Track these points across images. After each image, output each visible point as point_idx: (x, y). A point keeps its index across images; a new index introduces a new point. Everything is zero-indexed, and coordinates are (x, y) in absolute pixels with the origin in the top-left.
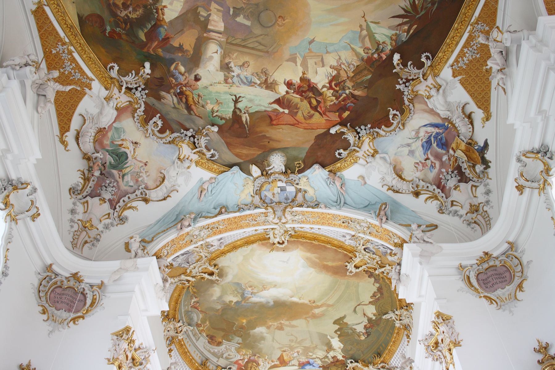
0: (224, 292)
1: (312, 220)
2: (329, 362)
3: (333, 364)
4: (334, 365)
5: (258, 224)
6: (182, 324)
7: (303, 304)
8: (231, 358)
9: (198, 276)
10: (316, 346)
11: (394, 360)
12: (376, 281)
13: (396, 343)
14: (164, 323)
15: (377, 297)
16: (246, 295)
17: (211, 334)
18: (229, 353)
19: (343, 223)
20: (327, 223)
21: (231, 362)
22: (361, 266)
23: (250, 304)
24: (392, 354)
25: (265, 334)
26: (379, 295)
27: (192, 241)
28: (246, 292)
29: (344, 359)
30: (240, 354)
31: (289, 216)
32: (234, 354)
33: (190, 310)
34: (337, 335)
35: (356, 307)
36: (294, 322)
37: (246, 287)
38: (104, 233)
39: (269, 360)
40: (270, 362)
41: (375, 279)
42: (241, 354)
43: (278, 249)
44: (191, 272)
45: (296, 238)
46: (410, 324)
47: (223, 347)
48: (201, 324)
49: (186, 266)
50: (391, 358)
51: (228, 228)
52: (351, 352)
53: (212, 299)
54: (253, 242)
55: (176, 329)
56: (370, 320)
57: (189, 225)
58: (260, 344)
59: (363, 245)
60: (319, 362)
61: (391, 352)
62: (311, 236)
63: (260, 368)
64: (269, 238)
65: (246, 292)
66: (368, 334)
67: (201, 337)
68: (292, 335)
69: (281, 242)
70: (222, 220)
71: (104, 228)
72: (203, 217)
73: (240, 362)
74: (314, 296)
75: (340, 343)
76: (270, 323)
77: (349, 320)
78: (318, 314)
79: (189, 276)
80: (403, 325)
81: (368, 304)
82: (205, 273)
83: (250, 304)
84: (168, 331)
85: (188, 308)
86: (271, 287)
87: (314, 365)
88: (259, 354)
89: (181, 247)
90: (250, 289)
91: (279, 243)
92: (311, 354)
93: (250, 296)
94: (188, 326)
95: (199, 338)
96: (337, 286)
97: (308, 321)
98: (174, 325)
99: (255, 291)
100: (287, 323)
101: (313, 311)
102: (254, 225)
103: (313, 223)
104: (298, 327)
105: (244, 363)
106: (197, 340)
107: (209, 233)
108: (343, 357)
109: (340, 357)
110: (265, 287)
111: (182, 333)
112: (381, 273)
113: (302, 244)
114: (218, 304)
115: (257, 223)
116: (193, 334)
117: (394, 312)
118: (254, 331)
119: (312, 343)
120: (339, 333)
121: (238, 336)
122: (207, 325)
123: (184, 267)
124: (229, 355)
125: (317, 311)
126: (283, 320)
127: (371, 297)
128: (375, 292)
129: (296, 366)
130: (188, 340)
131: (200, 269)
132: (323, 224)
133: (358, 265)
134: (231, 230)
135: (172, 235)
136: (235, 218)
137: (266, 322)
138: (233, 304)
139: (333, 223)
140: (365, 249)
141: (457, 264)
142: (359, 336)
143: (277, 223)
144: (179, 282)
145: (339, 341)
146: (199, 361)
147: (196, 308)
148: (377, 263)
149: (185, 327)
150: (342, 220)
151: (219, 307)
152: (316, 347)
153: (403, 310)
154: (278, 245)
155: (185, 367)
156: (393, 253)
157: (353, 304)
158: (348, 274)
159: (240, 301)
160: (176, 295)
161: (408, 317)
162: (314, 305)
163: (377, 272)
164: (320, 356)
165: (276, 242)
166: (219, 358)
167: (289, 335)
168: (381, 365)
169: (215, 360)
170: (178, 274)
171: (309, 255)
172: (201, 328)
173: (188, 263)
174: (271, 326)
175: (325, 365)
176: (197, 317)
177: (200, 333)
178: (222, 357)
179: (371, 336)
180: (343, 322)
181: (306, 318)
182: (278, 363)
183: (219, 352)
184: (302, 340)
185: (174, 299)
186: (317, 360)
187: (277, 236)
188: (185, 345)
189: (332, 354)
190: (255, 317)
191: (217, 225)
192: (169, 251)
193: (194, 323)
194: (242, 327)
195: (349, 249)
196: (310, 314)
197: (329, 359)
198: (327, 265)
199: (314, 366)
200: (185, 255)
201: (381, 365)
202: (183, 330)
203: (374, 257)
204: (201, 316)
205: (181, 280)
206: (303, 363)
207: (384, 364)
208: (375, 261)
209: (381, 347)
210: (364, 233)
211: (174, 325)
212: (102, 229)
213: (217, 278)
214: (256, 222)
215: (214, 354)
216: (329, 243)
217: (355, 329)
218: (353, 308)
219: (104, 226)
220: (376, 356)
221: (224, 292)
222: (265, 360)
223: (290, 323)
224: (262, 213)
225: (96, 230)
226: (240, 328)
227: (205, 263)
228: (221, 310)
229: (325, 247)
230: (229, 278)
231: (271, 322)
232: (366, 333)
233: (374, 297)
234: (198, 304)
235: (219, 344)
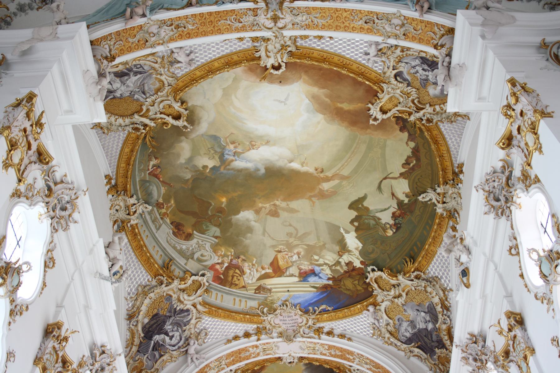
0: (195, 152)
1: (321, 22)
2: (342, 272)
3: (348, 274)
4: (349, 276)
5: (243, 29)
6: (136, 202)
7: (306, 174)
8: (206, 261)
9: (158, 119)
10: (324, 245)
11: (433, 266)
12: (411, 137)
13: (437, 241)
14: (110, 196)
15: (412, 165)
16: (226, 156)
17: (178, 220)
18: (203, 252)
19: (366, 23)
20: (342, 26)
21: (205, 266)
22: (390, 110)
23: (232, 171)
24: (430, 258)
25: (253, 223)
26: (414, 162)
27: (147, 41)
28: (227, 152)
29: (363, 266)
30: (217, 255)
31: (287, 18)
32: (209, 253)
33: (148, 179)
34: (354, 228)
35: (381, 181)
36: (294, 204)
37: (227, 143)
38: (18, 17)
39: (258, 266)
40: (260, 269)
41: (410, 135)
42: (219, 254)
43: (272, 80)
44: (148, 110)
45: (299, 59)
46: (457, 208)
47: (193, 243)
48: (163, 204)
49: (142, 100)
50: (429, 263)
51: (201, 30)
52: (373, 256)
53: (178, 162)
54: (236, 64)
55: (127, 207)
56: (400, 204)
57: (144, 15)
58: (246, 239)
59: (393, 70)
60: (328, 271)
61: (429, 255)
62: (319, 57)
63: (245, 279)
64: (260, 57)
65: (227, 152)
66: (397, 227)
67: (163, 225)
68: (290, 225)
69: (277, 64)
70: (192, 15)
71: (18, 9)
72: (164, 9)
73: (218, 267)
74: (323, 161)
75: (357, 241)
76: (260, 205)
77: (371, 204)
78: (327, 191)
79: (146, 117)
80: (447, 211)
81: (399, 177)
82: (168, 116)
83: (232, 171)
84: (117, 210)
85: (145, 175)
86: (262, 145)
87: (320, 275)
88: (245, 256)
89: (130, 47)
90: (232, 147)
91: (274, 67)
92: (316, 257)
93: (232, 158)
94: (145, 205)
95: (160, 226)
96: (355, 145)
97: (314, 203)
98: (125, 201)
99: (239, 150)
100: (283, 204)
101: (320, 187)
102: (238, 30)
103: (323, 28)
104: (297, 211)
105: (223, 269)
106: (158, 229)
107: (172, 33)
108: (362, 263)
109: (357, 264)
110: (254, 143)
111: (136, 215)
112: (418, 119)
113: (307, 69)
114: (188, 170)
115: (243, 27)
116: (151, 218)
117: (435, 190)
118: (238, 216)
119: (319, 239)
120: (356, 224)
121: (215, 225)
122: (171, 206)
123: (138, 100)
124: (202, 255)
125: (326, 186)
126: (277, 200)
127: (403, 165)
128: (409, 157)
129: (295, 276)
130: (144, 228)
131: (161, 106)
132: (337, 28)
133: (385, 108)
134: (205, 34)
135: (117, 26)
136: (210, 14)
137: (255, 201)
138: (208, 171)
139: (352, 26)
140: (396, 76)
141: (538, 40)
142: (385, 230)
143: (272, 28)
144: (131, 126)
145: (356, 237)
146: (160, 262)
147: (156, 176)
148: (413, 101)
149: (141, 207)
150: (364, 19)
151: (188, 176)
152: (323, 247)
153: (448, 186)
154: (272, 71)
155: (140, 269)
156: (439, 44)
157: (377, 176)
158: (371, 122)
159: (218, 165)
160: (127, 150)
161: (455, 198)
162: (322, 175)
163: (412, 118)
164: (329, 260)
165: (269, 66)
166: (187, 260)
167: (286, 226)
168: (415, 274)
169: (182, 261)
170: (130, 112)
171: (315, 90)
172: (164, 211)
173: (144, 93)
174: (261, 208)
175: (336, 277)
176: (158, 191)
177: (162, 218)
178: (192, 258)
179: (401, 230)
180: (362, 205)
181: (310, 198)
182: (270, 271)
183: (188, 249)
184: (305, 235)
185: (125, 157)
186: (325, 267)
187: (270, 54)
188: (140, 235)
189: (345, 258)
190: (239, 193)
191: (184, 22)
192: (112, 47)
193: (153, 201)
194: (220, 210)
195: (373, 78)
196: (317, 191)
197: (342, 267)
198: (341, 109)
199: (320, 278)
200: (139, 76)
201: (415, 274)
202: (138, 212)
203: (409, 91)
204: (163, 190)
205: (133, 124)
206: (305, 273)
207: (418, 273)
208: (410, 99)
209: (415, 247)
210: (396, 37)
211: (125, 201)
212: (15, 11)
213: (185, 123)
214: (241, 25)
215: (181, 253)
216: (344, 66)
217: (380, 219)
218: (377, 185)
219: (18, 7)
220: (408, 260)
221: (195, 152)
222: (253, 265)
223: (288, 205)
224: (250, 9)
225: (6, 10)
226: (218, 212)
227: (168, 96)
228: (191, 181)
229: (339, 74)
230: (203, 128)
231: (261, 203)
232: (395, 224)
233: (408, 166)
234: (159, 170)
235: (189, 237)
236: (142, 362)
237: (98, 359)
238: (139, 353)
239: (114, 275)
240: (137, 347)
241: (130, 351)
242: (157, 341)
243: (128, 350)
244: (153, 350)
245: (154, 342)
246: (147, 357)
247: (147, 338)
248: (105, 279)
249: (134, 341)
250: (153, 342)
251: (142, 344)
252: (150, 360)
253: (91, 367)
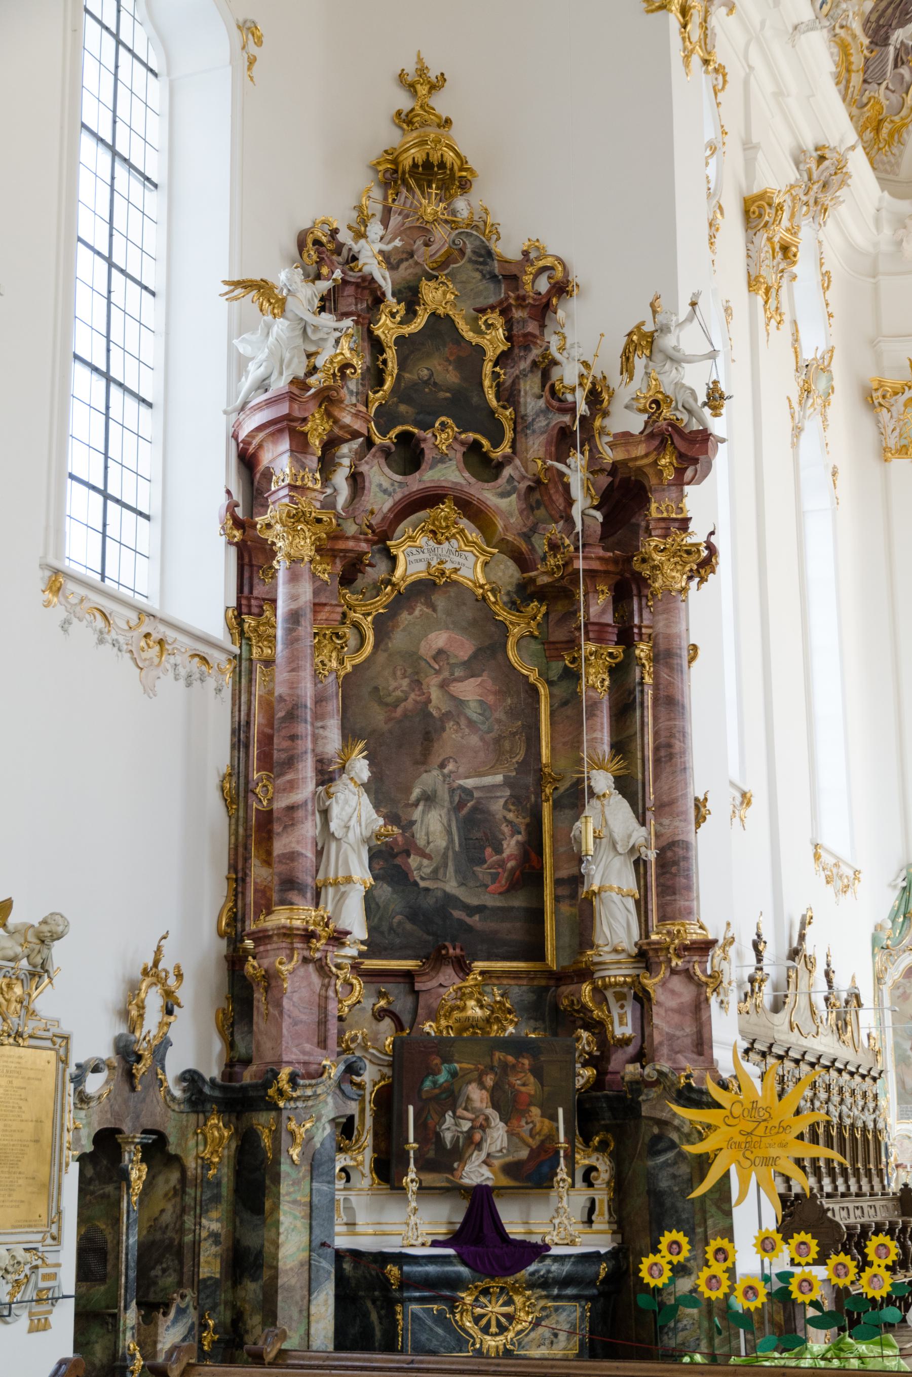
236: (878, 102)
237: (815, 176)
238: (866, 86)
239: (821, 7)
240: (861, 73)
241: (847, 88)
242: (902, 42)
243: (842, 86)
244: (896, 66)
245: (896, 48)
246: (887, 88)
247: (876, 44)
248: (808, 31)
249: (851, 63)
250: (891, 49)
251: (870, 63)
252: (893, 92)
253: (804, 198)
